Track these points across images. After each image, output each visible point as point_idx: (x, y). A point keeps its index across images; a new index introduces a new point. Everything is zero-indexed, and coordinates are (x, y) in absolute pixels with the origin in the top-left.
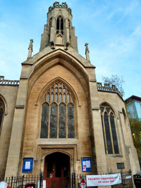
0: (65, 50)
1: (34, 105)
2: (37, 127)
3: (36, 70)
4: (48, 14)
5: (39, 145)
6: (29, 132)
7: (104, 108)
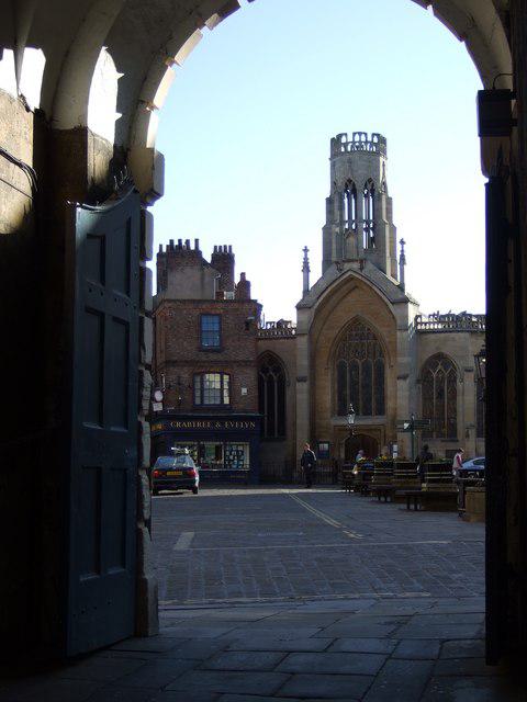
3: (318, 311)
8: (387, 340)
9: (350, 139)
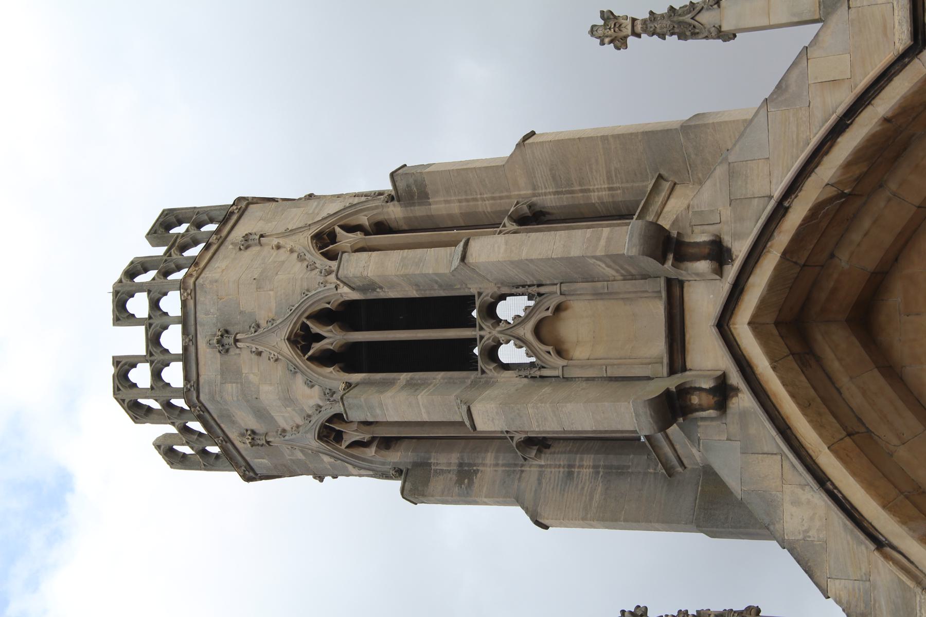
0: (732, 271)
4: (250, 474)
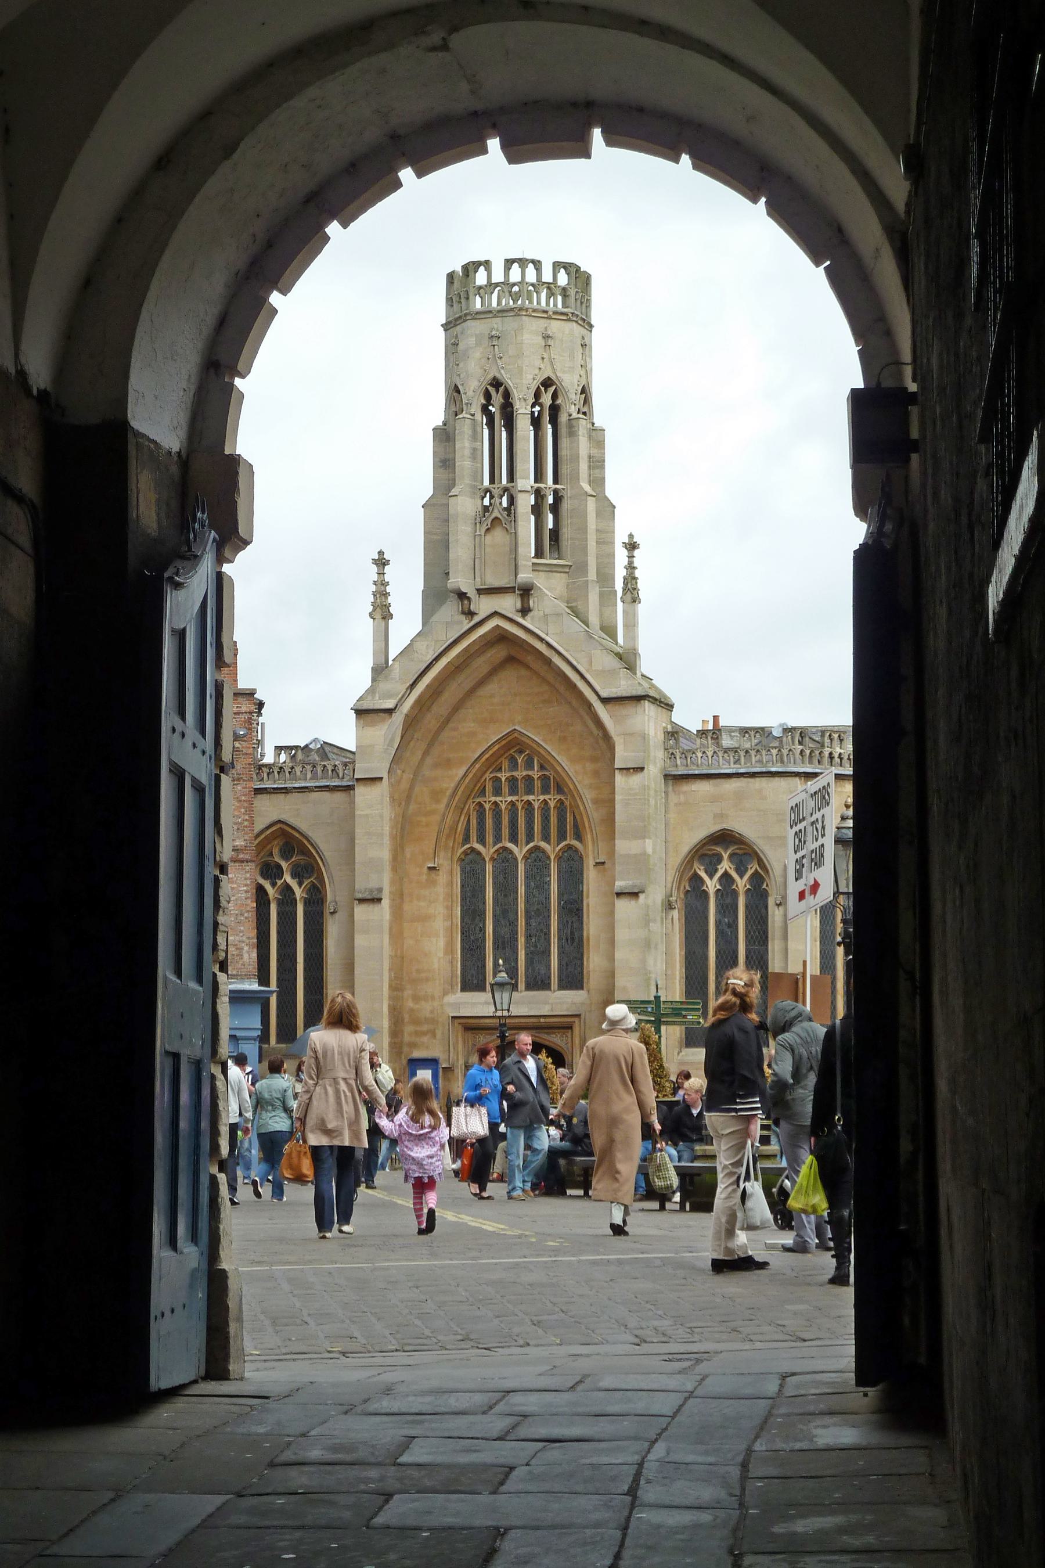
1: (425, 870)
2: (441, 954)
3: (411, 723)
5: (452, 1017)
6: (418, 971)
7: (720, 860)
8: (588, 795)
9: (498, 276)
